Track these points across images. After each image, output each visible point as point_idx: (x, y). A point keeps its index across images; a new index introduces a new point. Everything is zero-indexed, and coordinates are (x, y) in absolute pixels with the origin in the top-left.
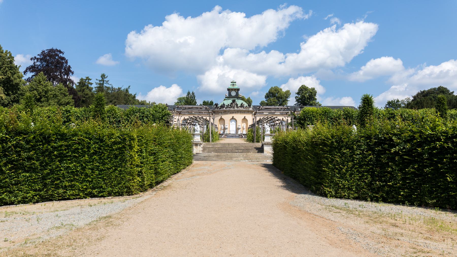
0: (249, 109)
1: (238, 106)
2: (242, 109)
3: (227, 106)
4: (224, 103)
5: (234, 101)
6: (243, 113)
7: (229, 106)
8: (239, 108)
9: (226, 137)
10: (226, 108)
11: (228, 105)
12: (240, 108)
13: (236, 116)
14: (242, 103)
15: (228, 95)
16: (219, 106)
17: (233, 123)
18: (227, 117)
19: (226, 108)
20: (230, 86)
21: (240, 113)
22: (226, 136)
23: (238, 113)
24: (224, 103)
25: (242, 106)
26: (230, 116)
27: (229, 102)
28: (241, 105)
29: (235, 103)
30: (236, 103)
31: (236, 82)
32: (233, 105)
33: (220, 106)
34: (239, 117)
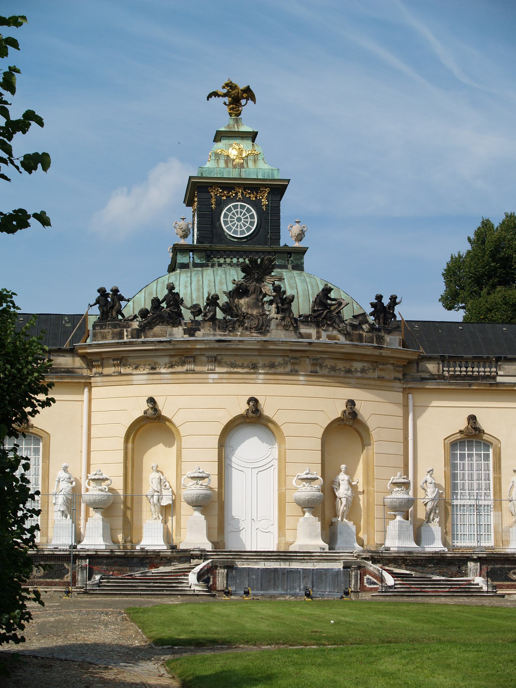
0: (380, 339)
2: (324, 339)
3: (196, 310)
4: (171, 288)
6: (333, 369)
7: (220, 315)
8: (304, 330)
9: (220, 582)
10: (191, 331)
11: (213, 301)
12: (313, 331)
14: (327, 290)
15: (192, 240)
19: (191, 331)
20: (210, 164)
21: (314, 373)
22: (221, 572)
23: (294, 372)
24: (171, 288)
29: (268, 288)
30: (277, 289)
31: (253, 136)
33: (144, 313)
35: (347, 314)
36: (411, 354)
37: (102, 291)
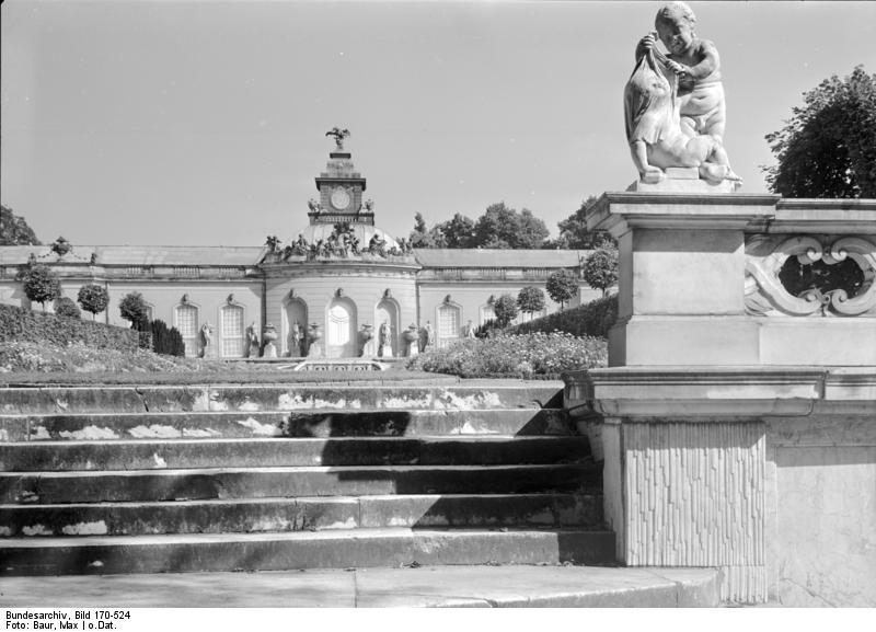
1: (360, 247)
5: (341, 228)
11: (320, 243)
13: (353, 284)
14: (376, 237)
16: (282, 246)
17: (341, 311)
18: (313, 289)
25: (375, 245)
26: (326, 284)
27: (324, 232)
28: (372, 242)
31: (349, 156)
32: (337, 244)
33: (288, 248)
34: (366, 288)
35: (387, 248)
36: (250, 276)
37: (269, 238)
